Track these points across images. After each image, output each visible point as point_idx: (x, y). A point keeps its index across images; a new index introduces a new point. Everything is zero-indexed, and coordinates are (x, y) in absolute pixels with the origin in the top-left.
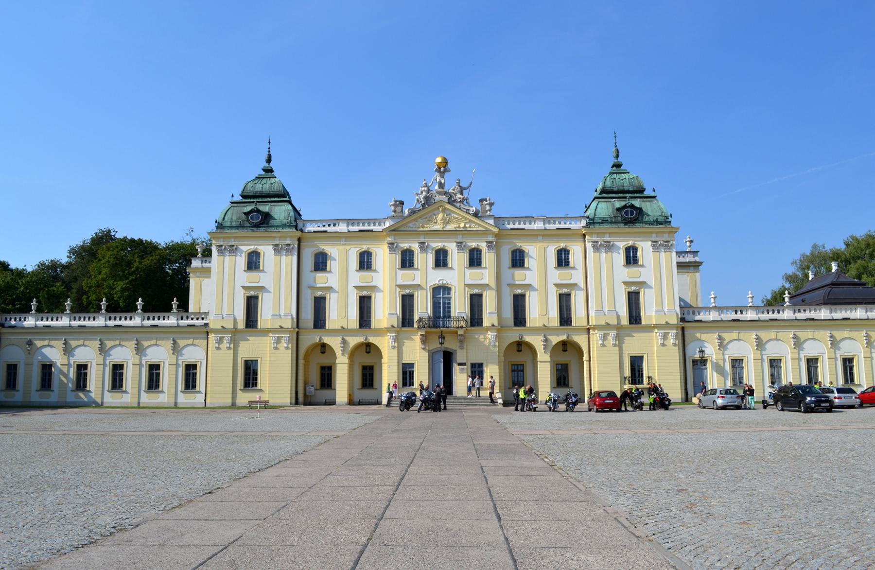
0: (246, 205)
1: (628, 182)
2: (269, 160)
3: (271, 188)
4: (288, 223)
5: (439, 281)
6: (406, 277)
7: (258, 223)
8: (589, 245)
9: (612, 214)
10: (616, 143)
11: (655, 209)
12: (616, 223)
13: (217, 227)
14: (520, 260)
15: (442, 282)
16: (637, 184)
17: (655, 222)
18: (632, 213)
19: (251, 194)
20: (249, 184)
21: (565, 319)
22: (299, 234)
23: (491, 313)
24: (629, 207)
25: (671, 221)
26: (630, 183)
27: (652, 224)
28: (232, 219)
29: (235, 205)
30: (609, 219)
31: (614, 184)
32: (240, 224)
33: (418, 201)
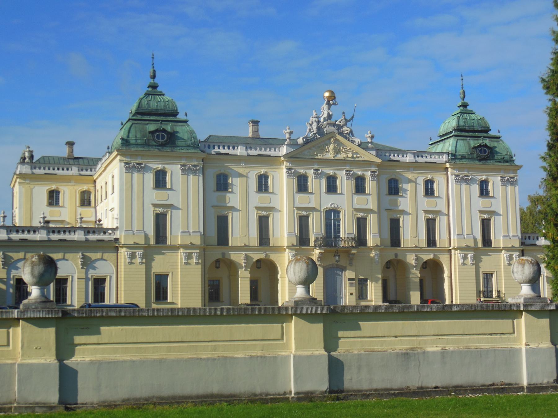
0: (147, 122)
1: (477, 122)
2: (154, 77)
3: (166, 107)
4: (192, 144)
5: (331, 205)
6: (301, 199)
7: (164, 143)
8: (451, 178)
9: (468, 151)
10: (463, 85)
11: (501, 149)
12: (472, 159)
13: (122, 144)
14: (394, 188)
15: (334, 206)
16: (484, 125)
17: (502, 160)
18: (485, 152)
19: (147, 111)
20: (143, 101)
21: (431, 242)
22: (204, 155)
23: (374, 235)
24: (483, 146)
25: (514, 160)
26: (478, 123)
27: (500, 162)
28: (136, 137)
29: (136, 122)
30: (467, 155)
31: (466, 123)
32: (145, 142)
33: (310, 130)
